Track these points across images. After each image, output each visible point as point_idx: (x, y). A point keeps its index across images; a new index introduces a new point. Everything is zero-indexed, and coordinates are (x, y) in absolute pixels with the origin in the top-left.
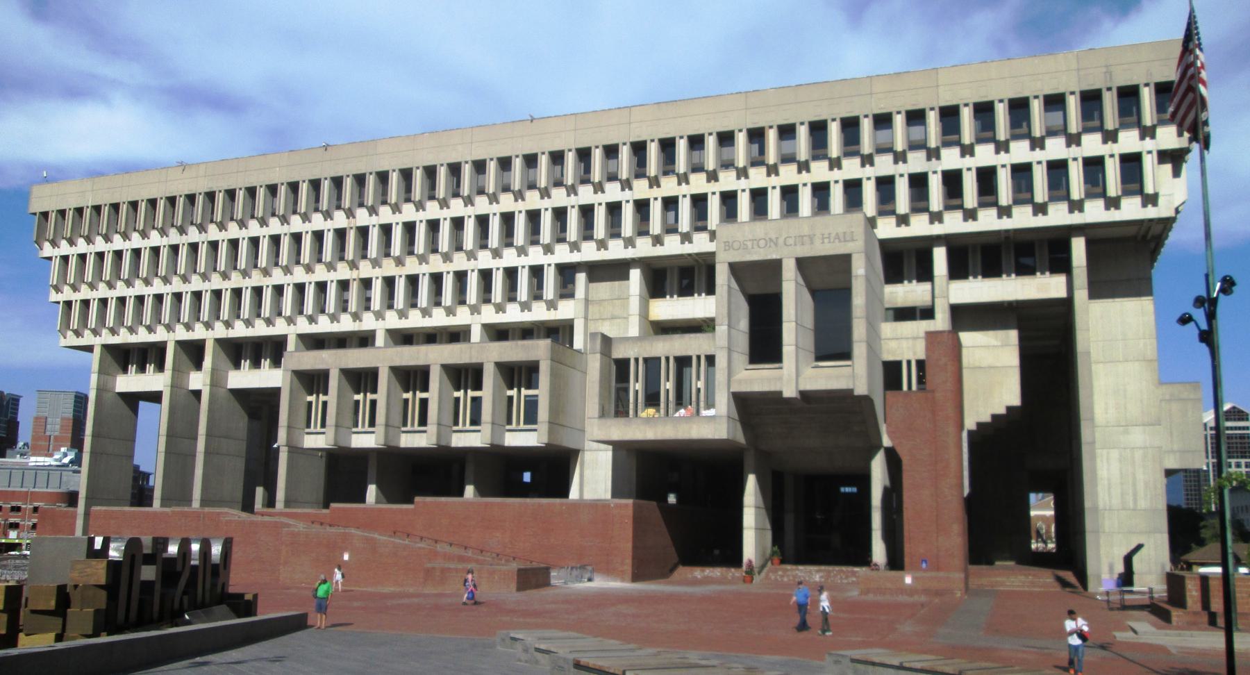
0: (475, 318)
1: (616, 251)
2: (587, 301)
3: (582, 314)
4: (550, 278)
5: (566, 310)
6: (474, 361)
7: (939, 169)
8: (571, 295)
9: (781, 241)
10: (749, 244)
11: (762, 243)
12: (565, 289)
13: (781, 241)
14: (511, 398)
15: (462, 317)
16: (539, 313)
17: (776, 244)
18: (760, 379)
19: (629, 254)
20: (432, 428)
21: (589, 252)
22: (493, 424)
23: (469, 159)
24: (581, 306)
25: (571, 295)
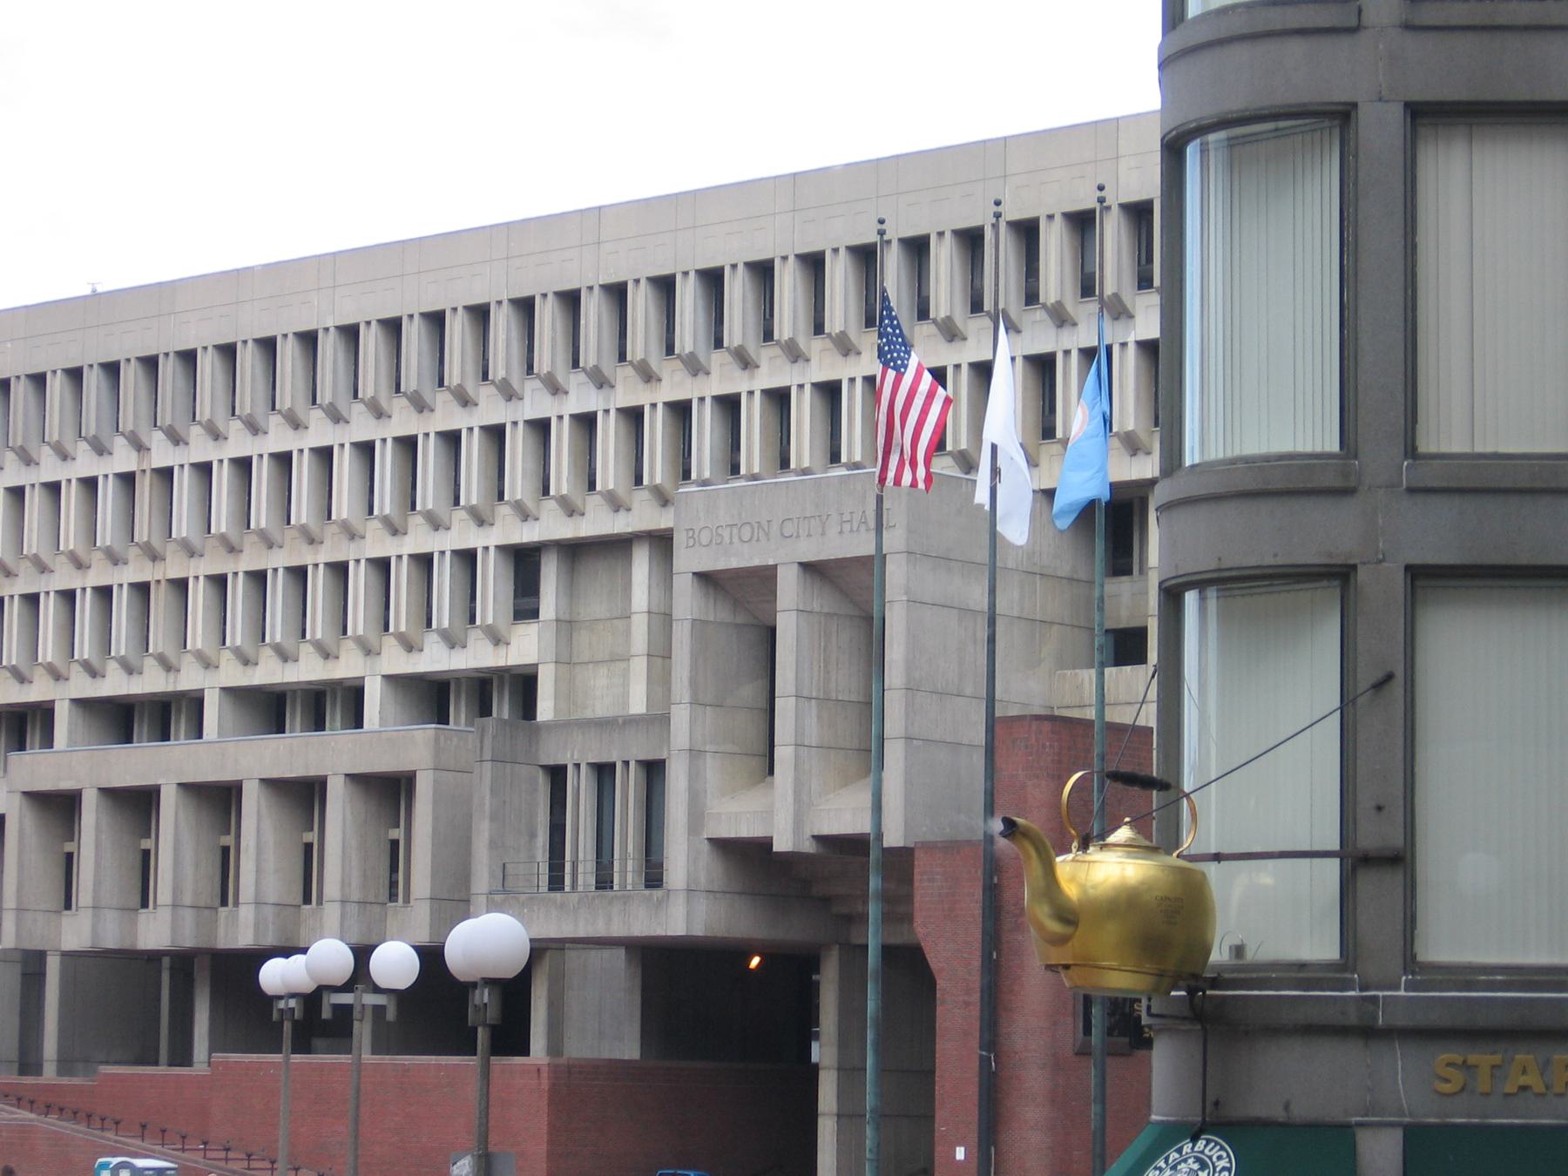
0: (374, 669)
1: (596, 522)
2: (567, 626)
3: (551, 656)
4: (493, 581)
5: (525, 646)
6: (312, 773)
7: (1131, 339)
8: (534, 614)
9: (775, 527)
10: (726, 533)
11: (746, 535)
12: (526, 609)
13: (775, 527)
14: (395, 844)
15: (347, 666)
16: (478, 656)
17: (767, 534)
18: (740, 816)
19: (620, 525)
20: (246, 913)
21: (551, 526)
22: (343, 902)
23: (330, 323)
24: (550, 635)
25: (534, 614)
